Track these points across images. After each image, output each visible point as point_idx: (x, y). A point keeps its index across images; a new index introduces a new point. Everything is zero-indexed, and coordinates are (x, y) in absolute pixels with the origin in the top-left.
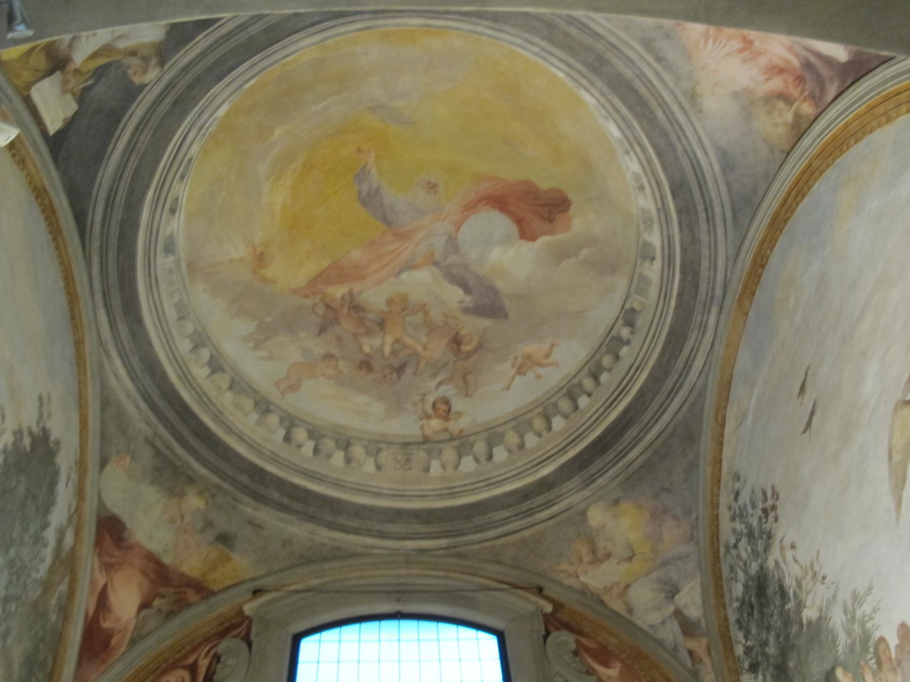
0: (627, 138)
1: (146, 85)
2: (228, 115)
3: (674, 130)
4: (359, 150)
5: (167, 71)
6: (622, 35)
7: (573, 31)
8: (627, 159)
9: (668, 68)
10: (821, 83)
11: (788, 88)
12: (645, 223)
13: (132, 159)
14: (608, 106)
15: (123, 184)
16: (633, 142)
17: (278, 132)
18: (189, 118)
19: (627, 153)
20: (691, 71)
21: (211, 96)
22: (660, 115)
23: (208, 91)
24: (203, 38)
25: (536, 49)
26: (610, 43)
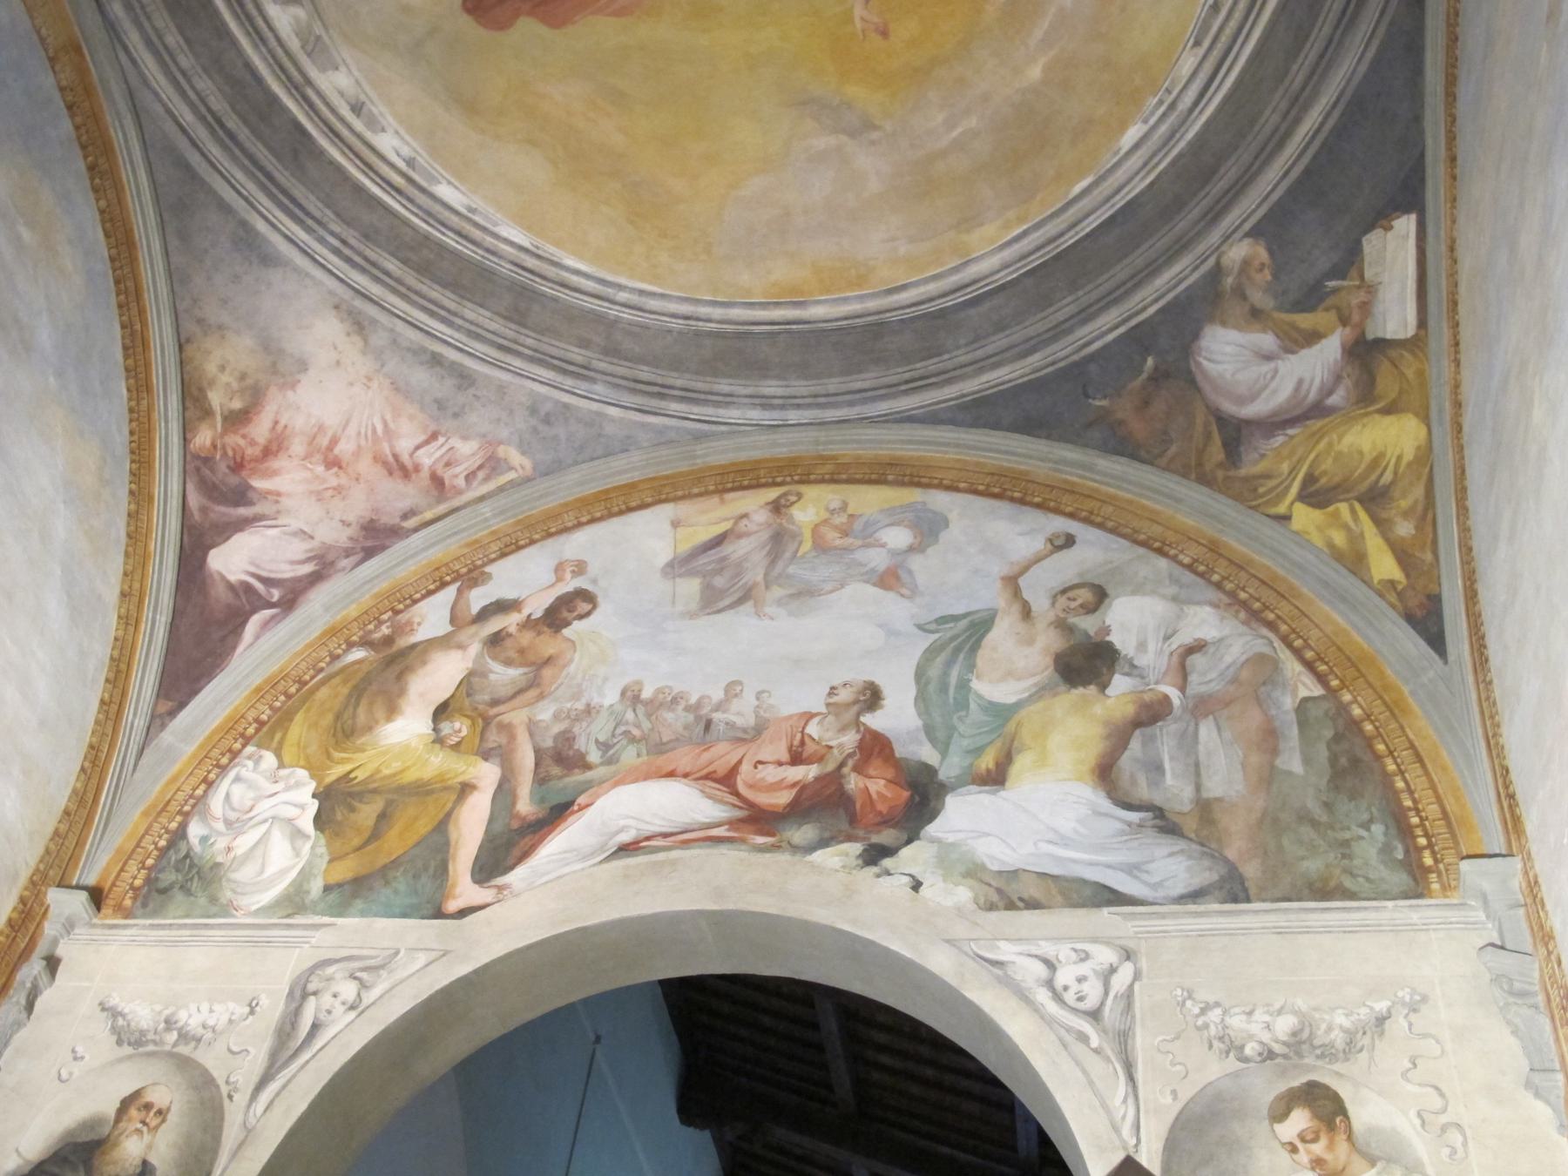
0: (423, 190)
1: (1247, 235)
2: (1123, 127)
3: (359, 254)
4: (884, 33)
5: (1212, 253)
6: (505, 377)
7: (577, 354)
8: (406, 151)
9: (417, 351)
10: (211, 490)
11: (244, 437)
12: (318, 38)
13: (1300, 78)
14: (477, 234)
15: (1327, 30)
16: (412, 188)
17: (1035, 73)
18: (1190, 135)
19: (410, 162)
20: (383, 366)
21: (1149, 173)
22: (392, 265)
23: (1152, 184)
24: (1144, 309)
25: (622, 296)
26: (518, 354)
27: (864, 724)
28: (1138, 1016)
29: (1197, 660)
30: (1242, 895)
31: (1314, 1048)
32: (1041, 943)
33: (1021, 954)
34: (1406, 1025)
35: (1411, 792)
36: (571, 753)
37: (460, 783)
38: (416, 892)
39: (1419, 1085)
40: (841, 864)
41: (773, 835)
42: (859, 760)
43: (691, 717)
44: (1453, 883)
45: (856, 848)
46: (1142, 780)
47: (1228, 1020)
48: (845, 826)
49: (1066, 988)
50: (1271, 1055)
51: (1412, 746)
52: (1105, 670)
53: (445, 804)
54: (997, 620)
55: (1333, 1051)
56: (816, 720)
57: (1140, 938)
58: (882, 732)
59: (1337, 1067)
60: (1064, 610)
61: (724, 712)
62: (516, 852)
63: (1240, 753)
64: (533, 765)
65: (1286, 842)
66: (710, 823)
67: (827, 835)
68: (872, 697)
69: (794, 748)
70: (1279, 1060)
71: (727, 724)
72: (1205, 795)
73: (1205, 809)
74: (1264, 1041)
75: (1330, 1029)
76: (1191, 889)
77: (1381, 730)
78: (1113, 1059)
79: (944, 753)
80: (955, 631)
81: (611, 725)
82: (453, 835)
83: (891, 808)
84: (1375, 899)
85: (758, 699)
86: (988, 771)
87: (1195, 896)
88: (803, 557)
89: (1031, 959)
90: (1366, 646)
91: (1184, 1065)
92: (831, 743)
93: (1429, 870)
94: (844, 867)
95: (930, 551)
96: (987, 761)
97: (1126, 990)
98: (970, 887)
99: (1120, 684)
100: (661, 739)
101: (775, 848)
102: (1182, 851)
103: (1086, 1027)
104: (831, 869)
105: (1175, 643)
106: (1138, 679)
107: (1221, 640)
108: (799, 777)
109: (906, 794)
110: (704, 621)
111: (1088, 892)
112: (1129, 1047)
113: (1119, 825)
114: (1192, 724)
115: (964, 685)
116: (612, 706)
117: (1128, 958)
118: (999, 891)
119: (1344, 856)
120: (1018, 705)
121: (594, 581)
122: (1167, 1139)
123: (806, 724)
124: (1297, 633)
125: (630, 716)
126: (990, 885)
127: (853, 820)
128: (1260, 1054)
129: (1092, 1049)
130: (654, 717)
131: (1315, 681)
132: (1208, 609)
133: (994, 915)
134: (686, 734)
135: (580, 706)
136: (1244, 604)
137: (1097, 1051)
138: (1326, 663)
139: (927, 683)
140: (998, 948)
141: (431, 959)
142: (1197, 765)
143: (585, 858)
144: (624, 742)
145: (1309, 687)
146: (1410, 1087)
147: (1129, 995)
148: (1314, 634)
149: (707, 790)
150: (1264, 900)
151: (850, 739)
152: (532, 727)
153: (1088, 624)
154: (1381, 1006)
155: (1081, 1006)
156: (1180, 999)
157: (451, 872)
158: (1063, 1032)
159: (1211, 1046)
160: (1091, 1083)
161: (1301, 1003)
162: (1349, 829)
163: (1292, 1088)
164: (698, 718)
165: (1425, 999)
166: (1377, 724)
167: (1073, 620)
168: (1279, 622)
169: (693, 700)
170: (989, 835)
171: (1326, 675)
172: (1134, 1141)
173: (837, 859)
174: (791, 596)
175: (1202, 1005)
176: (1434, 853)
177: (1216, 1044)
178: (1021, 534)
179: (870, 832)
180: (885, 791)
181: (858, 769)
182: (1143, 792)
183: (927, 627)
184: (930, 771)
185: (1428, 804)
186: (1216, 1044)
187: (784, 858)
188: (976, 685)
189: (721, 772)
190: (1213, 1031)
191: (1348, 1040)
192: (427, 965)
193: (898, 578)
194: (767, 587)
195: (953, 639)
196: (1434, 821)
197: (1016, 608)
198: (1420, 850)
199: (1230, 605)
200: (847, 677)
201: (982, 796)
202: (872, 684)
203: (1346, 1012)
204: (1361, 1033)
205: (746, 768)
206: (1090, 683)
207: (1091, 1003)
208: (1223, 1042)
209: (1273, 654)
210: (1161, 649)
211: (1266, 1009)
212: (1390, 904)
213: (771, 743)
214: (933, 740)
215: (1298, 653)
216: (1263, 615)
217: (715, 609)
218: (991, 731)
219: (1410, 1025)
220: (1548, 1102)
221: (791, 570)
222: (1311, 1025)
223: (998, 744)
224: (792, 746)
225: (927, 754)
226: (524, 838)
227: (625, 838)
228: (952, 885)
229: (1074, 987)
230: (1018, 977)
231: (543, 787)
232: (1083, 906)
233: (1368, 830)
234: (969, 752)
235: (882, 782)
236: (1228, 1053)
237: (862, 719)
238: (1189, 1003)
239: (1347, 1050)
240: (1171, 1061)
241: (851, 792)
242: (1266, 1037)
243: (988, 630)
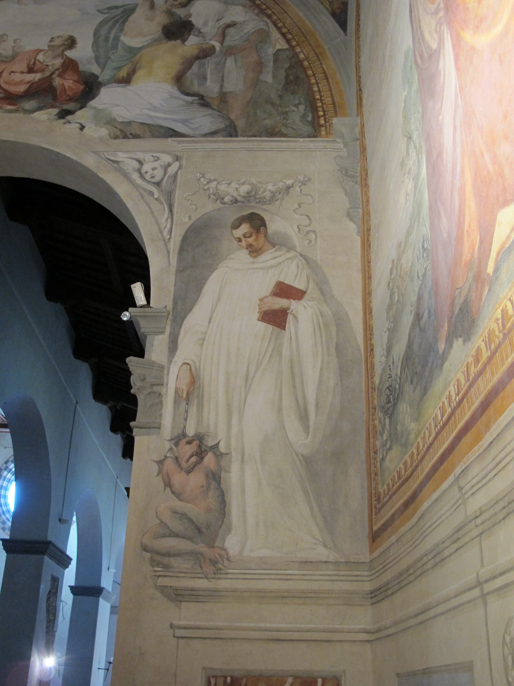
27: (66, 55)
28: (178, 184)
29: (231, 31)
30: (234, 134)
31: (256, 198)
32: (138, 153)
33: (128, 158)
34: (299, 190)
35: (320, 91)
39: (301, 215)
42: (60, 72)
44: (331, 132)
45: (55, 111)
46: (196, 83)
47: (219, 187)
49: (146, 173)
50: (236, 201)
51: (325, 73)
52: (186, 33)
54: (138, 9)
55: (264, 200)
56: (42, 53)
57: (184, 151)
59: (265, 207)
60: (171, 5)
63: (244, 73)
65: (258, 112)
67: (42, 105)
68: (71, 43)
69: (30, 66)
70: (240, 204)
72: (224, 90)
73: (223, 97)
74: (234, 196)
75: (265, 191)
76: (211, 131)
77: (311, 65)
78: (164, 203)
79: (103, 67)
84: (295, 137)
86: (123, 77)
87: (213, 134)
89: (132, 160)
90: (311, 27)
91: (196, 205)
92: (50, 64)
93: (322, 126)
94: (48, 120)
96: (123, 73)
97: (174, 174)
99: (192, 40)
101: (16, 111)
102: (209, 114)
103: (153, 189)
105: (223, 22)
106: (201, 38)
107: (245, 21)
108: (31, 79)
109: (82, 87)
111: (162, 131)
112: (172, 198)
113: (181, 102)
114: (224, 58)
115: (117, 39)
117: (177, 160)
118: (121, 130)
119: (284, 119)
122: (184, 236)
123: (37, 55)
124: (281, 20)
126: (116, 128)
128: (231, 201)
129: (154, 198)
131: (285, 42)
132: (240, 8)
133: (117, 141)
136: (258, 6)
137: (156, 199)
138: (292, 34)
142: (223, 77)
145: (282, 44)
146: (296, 216)
147: (175, 176)
148: (289, 21)
150: (244, 136)
151: (58, 62)
153: (181, 12)
154: (289, 182)
155: (153, 180)
156: (198, 177)
158: (142, 191)
159: (209, 197)
160: (152, 213)
161: (253, 180)
162: (288, 107)
163: (244, 215)
165: (309, 180)
166: (310, 62)
167: (174, 10)
168: (273, 15)
171: (290, 40)
172: (169, 237)
173: (45, 116)
175: (208, 180)
176: (325, 119)
177: (212, 197)
180: (71, 85)
181: (60, 76)
182: (196, 88)
183: (102, 11)
184: (96, 77)
185: (327, 98)
186: (212, 197)
188: (123, 38)
190: (211, 191)
191: (272, 196)
195: (114, 17)
196: (328, 105)
198: (319, 117)
199: (251, 6)
201: (118, 88)
203: (273, 184)
204: (278, 193)
206: (178, 39)
207: (156, 180)
208: (215, 196)
209: (268, 30)
210: (215, 25)
211: (237, 182)
212: (301, 140)
215: (279, 29)
216: (266, 11)
219: (301, 190)
220: (354, 222)
222: (256, 189)
224: (29, 65)
225: (95, 69)
228: (99, 128)
229: (150, 172)
230: (125, 168)
232: (159, 137)
233: (297, 108)
235: (71, 81)
236: (216, 200)
237: (65, 53)
238: (202, 179)
239: (271, 200)
240: (190, 203)
242: (235, 194)
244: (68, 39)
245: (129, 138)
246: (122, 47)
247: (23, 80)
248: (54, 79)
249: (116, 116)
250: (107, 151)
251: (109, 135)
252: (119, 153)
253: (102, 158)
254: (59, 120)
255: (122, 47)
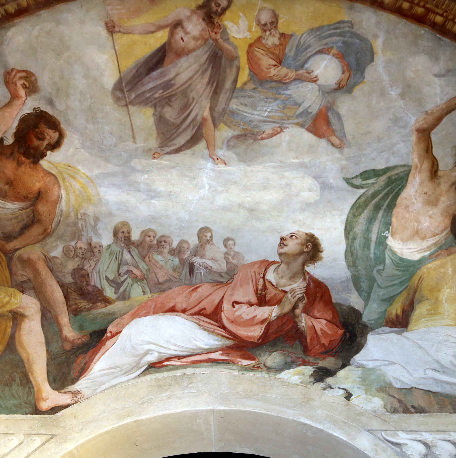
27: (308, 273)
32: (423, 433)
36: (90, 288)
37: (10, 312)
38: (14, 396)
40: (300, 381)
41: (254, 359)
42: (306, 304)
43: (176, 261)
45: (309, 370)
48: (300, 354)
53: (6, 329)
54: (410, 178)
56: (272, 268)
58: (322, 281)
61: (202, 257)
62: (75, 368)
64: (63, 298)
66: (208, 349)
67: (289, 360)
69: (259, 292)
71: (206, 268)
79: (367, 300)
80: (377, 187)
81: (114, 266)
82: (24, 355)
83: (331, 341)
85: (226, 246)
86: (397, 316)
88: (242, 89)
92: (287, 289)
94: (301, 382)
95: (357, 91)
98: (382, 398)
100: (158, 281)
101: (256, 368)
104: (294, 384)
108: (266, 316)
109: (341, 332)
110: (166, 161)
116: (109, 246)
118: (400, 401)
120: (421, 262)
121: (51, 103)
123: (266, 271)
125: (127, 257)
126: (394, 397)
127: (306, 350)
130: (147, 259)
133: (396, 416)
134: (174, 274)
135: (82, 244)
139: (354, 239)
140: (398, 435)
141: (44, 440)
143: (127, 373)
144: (129, 280)
149: (201, 323)
152: (48, 260)
157: (34, 383)
164: (182, 262)
169: (175, 245)
170: (396, 364)
173: (297, 377)
174: (238, 137)
178: (436, 76)
179: (317, 359)
180: (326, 329)
181: (306, 311)
184: (357, 314)
187: (262, 375)
189: (209, 309)
192: (43, 444)
193: (328, 123)
194: (215, 125)
195: (374, 196)
197: (426, 165)
200: (294, 229)
201: (392, 335)
202: (312, 236)
205: (226, 306)
213: (241, 286)
214: (358, 289)
217: (173, 148)
218: (402, 283)
221: (234, 105)
223: (405, 294)
224: (257, 290)
226: (78, 357)
227: (152, 358)
228: (370, 397)
231: (78, 317)
234: (384, 300)
235: (324, 322)
241: (302, 328)
243: (404, 187)
244: (307, 243)
245: (411, 412)
246: (392, 259)
247: (254, 317)
248: (298, 317)
249: (392, 380)
250: (385, 430)
251: (385, 406)
252: (400, 432)
253: (379, 439)
254: (317, 384)
255: (392, 259)
